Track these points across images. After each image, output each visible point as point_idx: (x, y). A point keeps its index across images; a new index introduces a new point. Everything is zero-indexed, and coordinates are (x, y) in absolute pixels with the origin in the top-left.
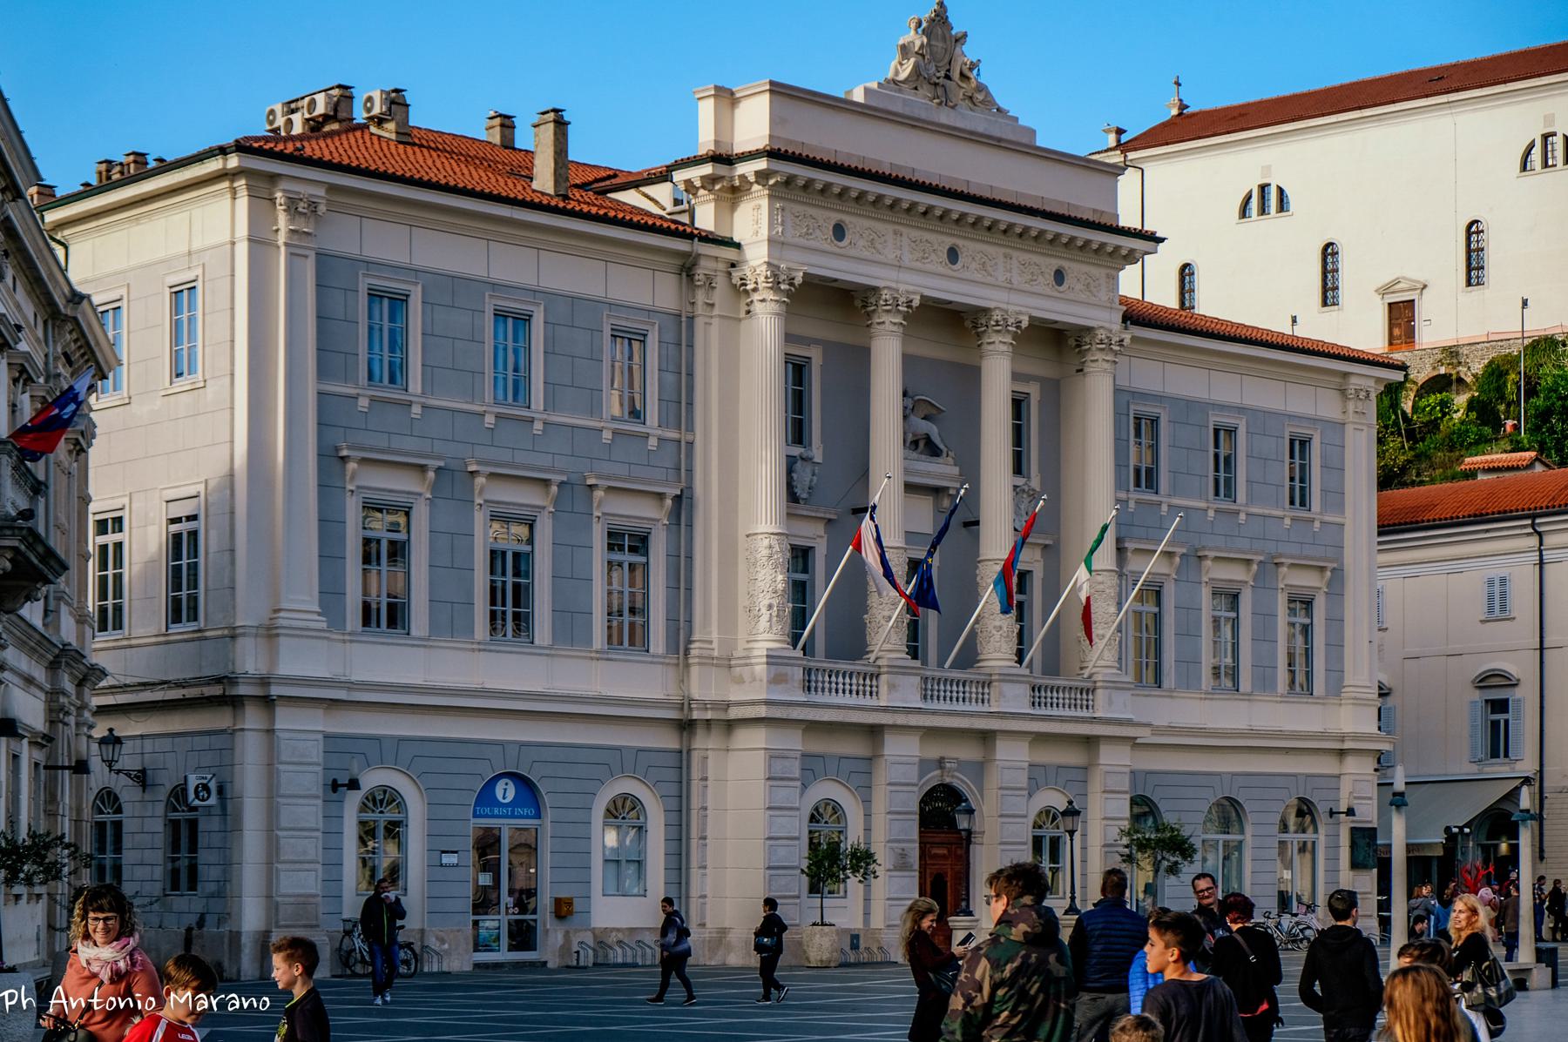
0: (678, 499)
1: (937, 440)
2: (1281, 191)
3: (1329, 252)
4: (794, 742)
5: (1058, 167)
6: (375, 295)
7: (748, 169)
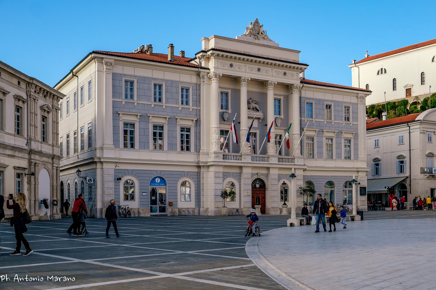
0: (197, 121)
1: (258, 108)
2: (385, 69)
3: (394, 80)
4: (221, 169)
5: (285, 51)
6: (126, 81)
7: (209, 53)
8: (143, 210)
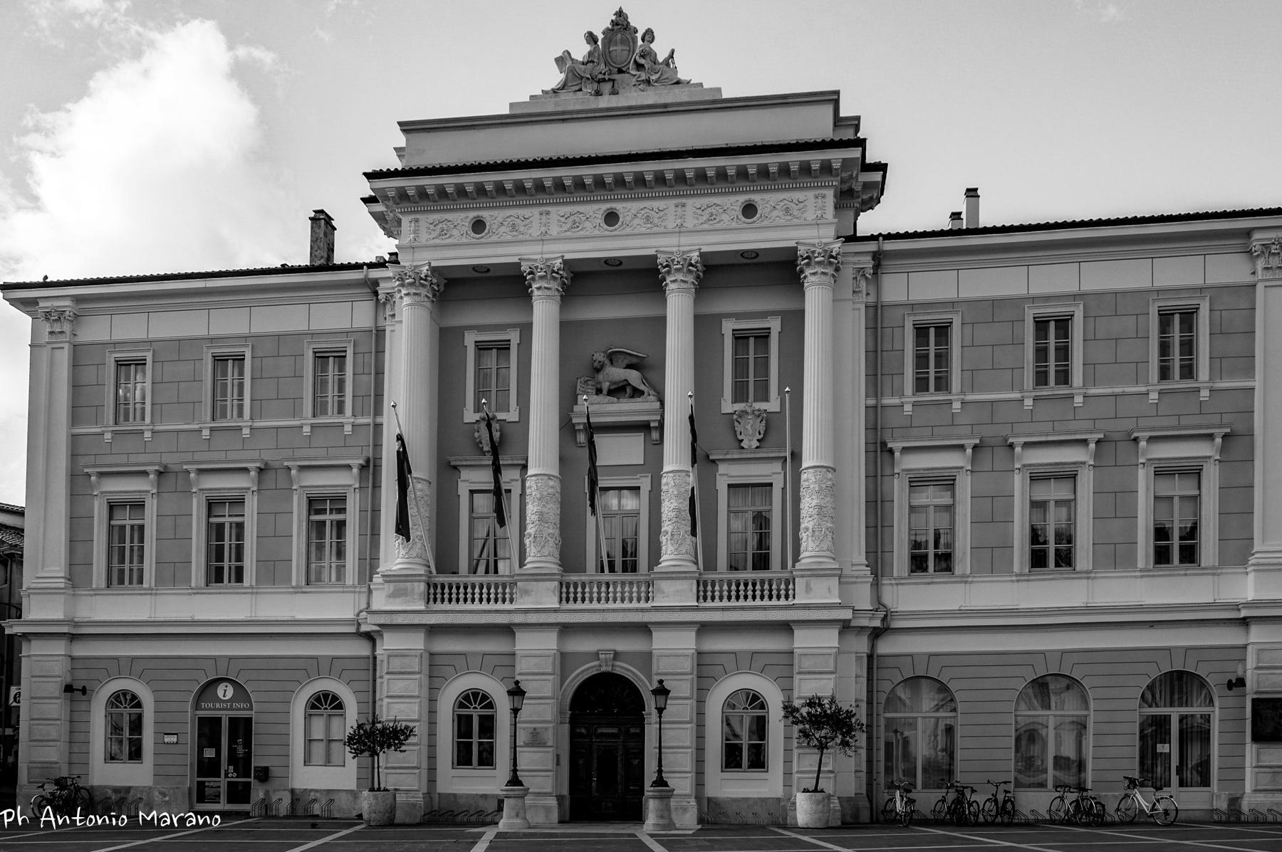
8: (164, 795)
